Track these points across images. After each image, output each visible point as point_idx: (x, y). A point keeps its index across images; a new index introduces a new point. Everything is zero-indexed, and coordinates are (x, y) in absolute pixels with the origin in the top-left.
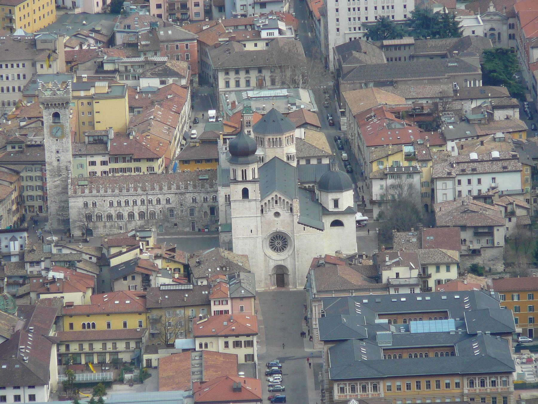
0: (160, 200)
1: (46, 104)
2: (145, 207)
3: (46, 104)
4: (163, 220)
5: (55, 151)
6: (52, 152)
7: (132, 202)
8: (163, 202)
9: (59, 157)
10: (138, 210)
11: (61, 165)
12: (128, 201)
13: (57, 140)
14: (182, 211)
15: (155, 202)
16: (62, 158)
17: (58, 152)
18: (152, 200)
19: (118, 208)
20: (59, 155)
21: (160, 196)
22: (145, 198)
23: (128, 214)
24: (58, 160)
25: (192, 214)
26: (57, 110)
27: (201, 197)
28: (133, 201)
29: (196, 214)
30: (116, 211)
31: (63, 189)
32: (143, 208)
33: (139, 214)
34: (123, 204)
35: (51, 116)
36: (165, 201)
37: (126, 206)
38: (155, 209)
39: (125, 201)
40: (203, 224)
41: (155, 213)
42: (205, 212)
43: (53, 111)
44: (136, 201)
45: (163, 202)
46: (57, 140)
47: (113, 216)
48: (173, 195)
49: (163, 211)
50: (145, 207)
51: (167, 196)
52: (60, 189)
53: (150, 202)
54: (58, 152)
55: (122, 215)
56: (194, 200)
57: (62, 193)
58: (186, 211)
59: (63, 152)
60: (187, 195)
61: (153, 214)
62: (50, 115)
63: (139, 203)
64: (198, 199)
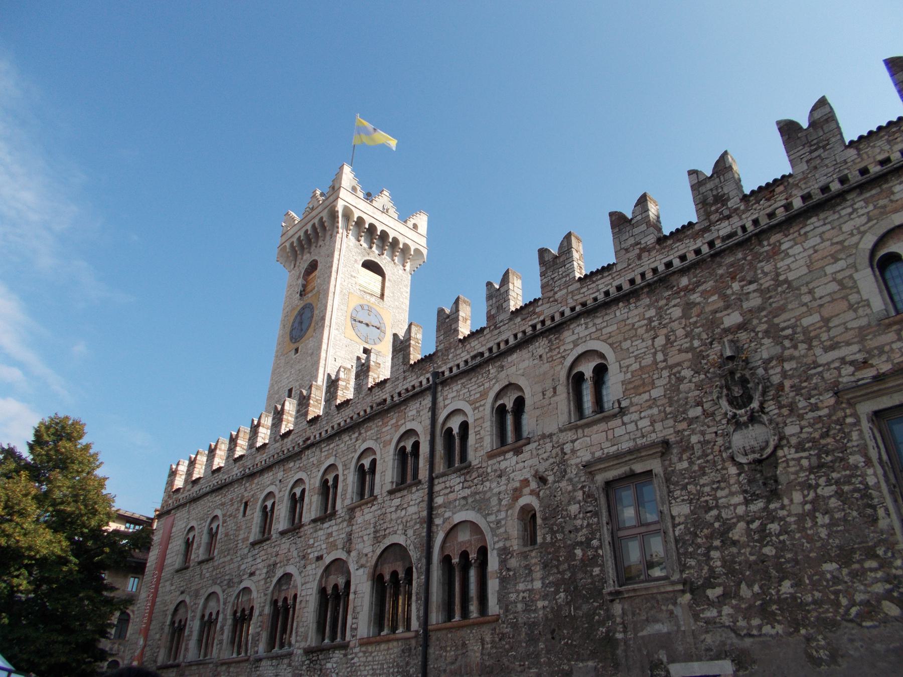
0: (520, 403)
2: (414, 502)
4: (557, 622)
8: (548, 413)
10: (377, 540)
14: (763, 472)
19: (285, 545)
23: (322, 591)
33: (377, 580)
36: (562, 400)
38: (481, 504)
41: (483, 552)
45: (548, 413)
46: (297, 350)
50: (414, 502)
51: (581, 338)
55: (295, 596)
58: (827, 458)
63: (386, 474)
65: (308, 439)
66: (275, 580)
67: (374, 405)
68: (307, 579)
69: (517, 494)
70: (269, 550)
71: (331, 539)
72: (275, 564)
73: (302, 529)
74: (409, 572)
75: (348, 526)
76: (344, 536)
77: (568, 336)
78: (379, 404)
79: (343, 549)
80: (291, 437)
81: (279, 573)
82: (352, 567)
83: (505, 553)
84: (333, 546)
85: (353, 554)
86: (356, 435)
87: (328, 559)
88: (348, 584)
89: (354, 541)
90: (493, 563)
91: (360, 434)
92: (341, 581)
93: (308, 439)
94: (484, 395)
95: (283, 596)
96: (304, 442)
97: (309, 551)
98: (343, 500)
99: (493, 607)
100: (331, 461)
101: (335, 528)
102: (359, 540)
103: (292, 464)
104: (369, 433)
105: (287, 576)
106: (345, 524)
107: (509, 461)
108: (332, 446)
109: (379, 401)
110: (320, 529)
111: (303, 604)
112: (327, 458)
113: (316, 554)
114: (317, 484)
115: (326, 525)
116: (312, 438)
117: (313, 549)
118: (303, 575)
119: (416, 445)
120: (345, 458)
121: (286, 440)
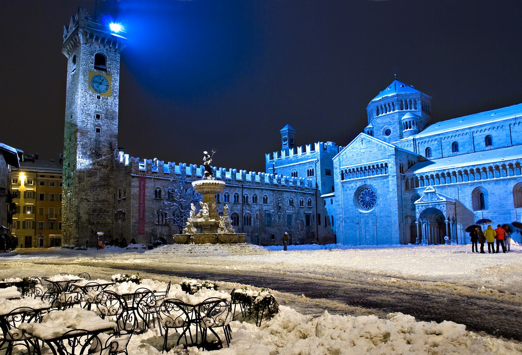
0: (256, 197)
2: (239, 207)
5: (93, 114)
6: (89, 115)
7: (223, 197)
8: (260, 201)
9: (99, 125)
11: (102, 139)
13: (99, 97)
15: (250, 200)
16: (104, 128)
18: (247, 197)
20: (100, 122)
21: (257, 192)
22: (240, 193)
24: (98, 131)
25: (289, 223)
27: (297, 199)
29: (293, 223)
31: (102, 179)
32: (238, 209)
35: (93, 57)
38: (251, 211)
40: (299, 237)
41: (250, 218)
42: (302, 220)
44: (228, 196)
45: (260, 201)
46: (99, 97)
48: (271, 193)
49: (261, 215)
52: (98, 179)
53: (245, 200)
54: (98, 117)
56: (291, 203)
57: (100, 186)
59: (106, 118)
60: (285, 195)
61: (248, 220)
62: (91, 54)
63: (232, 199)
64: (295, 200)
69: (256, 211)
74: (238, 218)
77: (264, 191)
83: (254, 219)
90: (252, 219)
94: (251, 194)
99: (252, 224)
107: (255, 206)
119: (238, 196)
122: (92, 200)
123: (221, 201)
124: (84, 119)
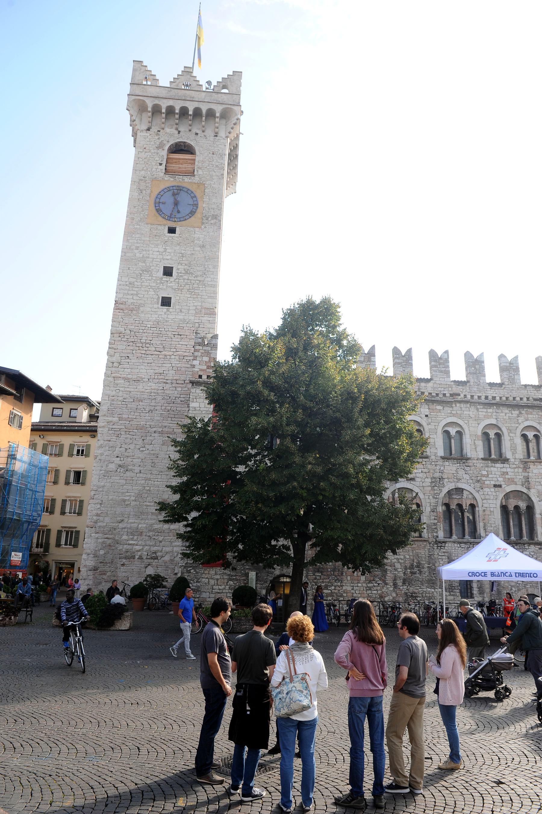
1: (150, 104)
3: (150, 104)
7: (519, 442)
12: (498, 436)
17: (168, 272)
19: (450, 468)
23: (504, 508)
26: (186, 137)
28: (524, 436)
30: (437, 482)
34: (474, 448)
37: (488, 458)
39: (486, 435)
43: (171, 135)
47: (426, 509)
54: (168, 272)
65: (459, 395)
66: (445, 490)
67: (531, 398)
68: (487, 497)
70: (429, 466)
71: (507, 476)
72: (441, 479)
73: (470, 461)
75: (523, 472)
76: (522, 477)
78: (535, 400)
79: (522, 485)
80: (430, 384)
81: (449, 486)
82: (534, 499)
84: (512, 481)
85: (532, 490)
86: (517, 412)
87: (509, 489)
88: (530, 508)
89: (532, 483)
91: (520, 413)
92: (523, 505)
93: (459, 395)
95: (456, 502)
96: (451, 395)
97: (484, 479)
98: (513, 454)
100: (494, 422)
101: (509, 470)
102: (537, 484)
103: (439, 407)
104: (529, 416)
105: (459, 491)
106: (520, 470)
108: (489, 410)
109: (535, 397)
110: (492, 466)
111: (487, 512)
112: (487, 417)
113: (493, 483)
114: (480, 433)
115: (498, 465)
116: (462, 396)
117: (487, 479)
118: (481, 493)
120: (509, 425)
121: (423, 384)
122: (137, 469)
123: (508, 454)
124: (132, 280)
